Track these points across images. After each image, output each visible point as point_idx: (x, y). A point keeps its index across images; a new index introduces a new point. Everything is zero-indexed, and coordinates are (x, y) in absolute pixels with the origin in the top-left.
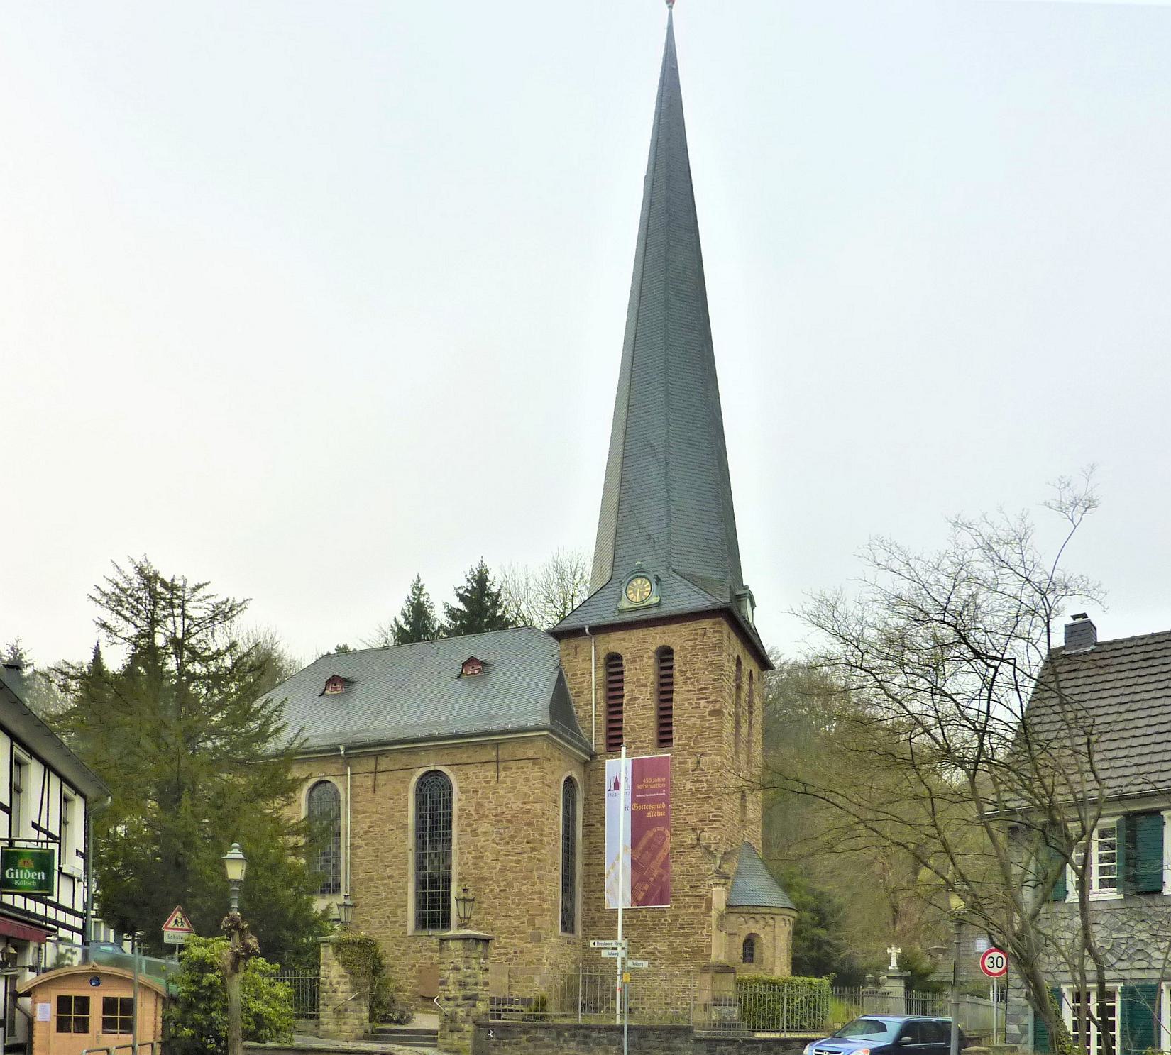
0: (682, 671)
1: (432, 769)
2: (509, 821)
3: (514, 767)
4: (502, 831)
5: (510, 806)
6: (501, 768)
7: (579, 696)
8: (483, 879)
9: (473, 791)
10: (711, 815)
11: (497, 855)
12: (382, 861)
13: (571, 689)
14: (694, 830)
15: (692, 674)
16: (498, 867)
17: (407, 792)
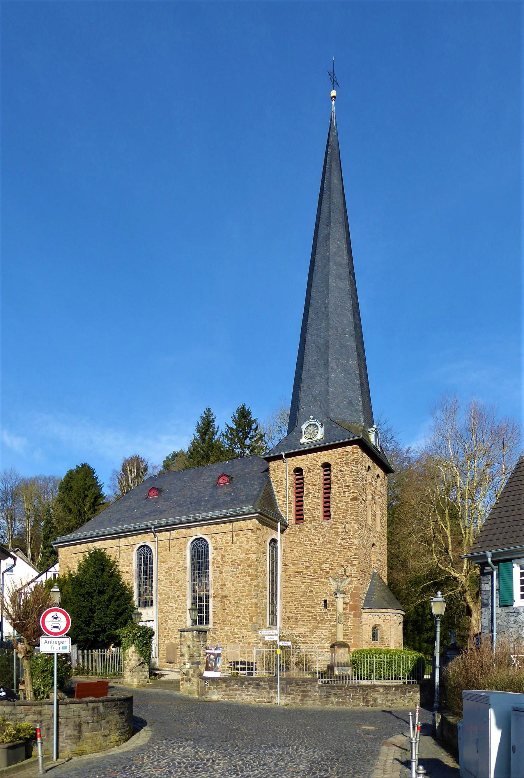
0: (335, 476)
1: (199, 537)
2: (238, 565)
3: (241, 534)
4: (235, 570)
5: (239, 556)
6: (234, 535)
7: (280, 493)
8: (226, 597)
9: (220, 549)
10: (352, 557)
11: (233, 584)
12: (174, 588)
13: (276, 489)
14: (343, 566)
15: (341, 477)
16: (234, 590)
17: (185, 550)
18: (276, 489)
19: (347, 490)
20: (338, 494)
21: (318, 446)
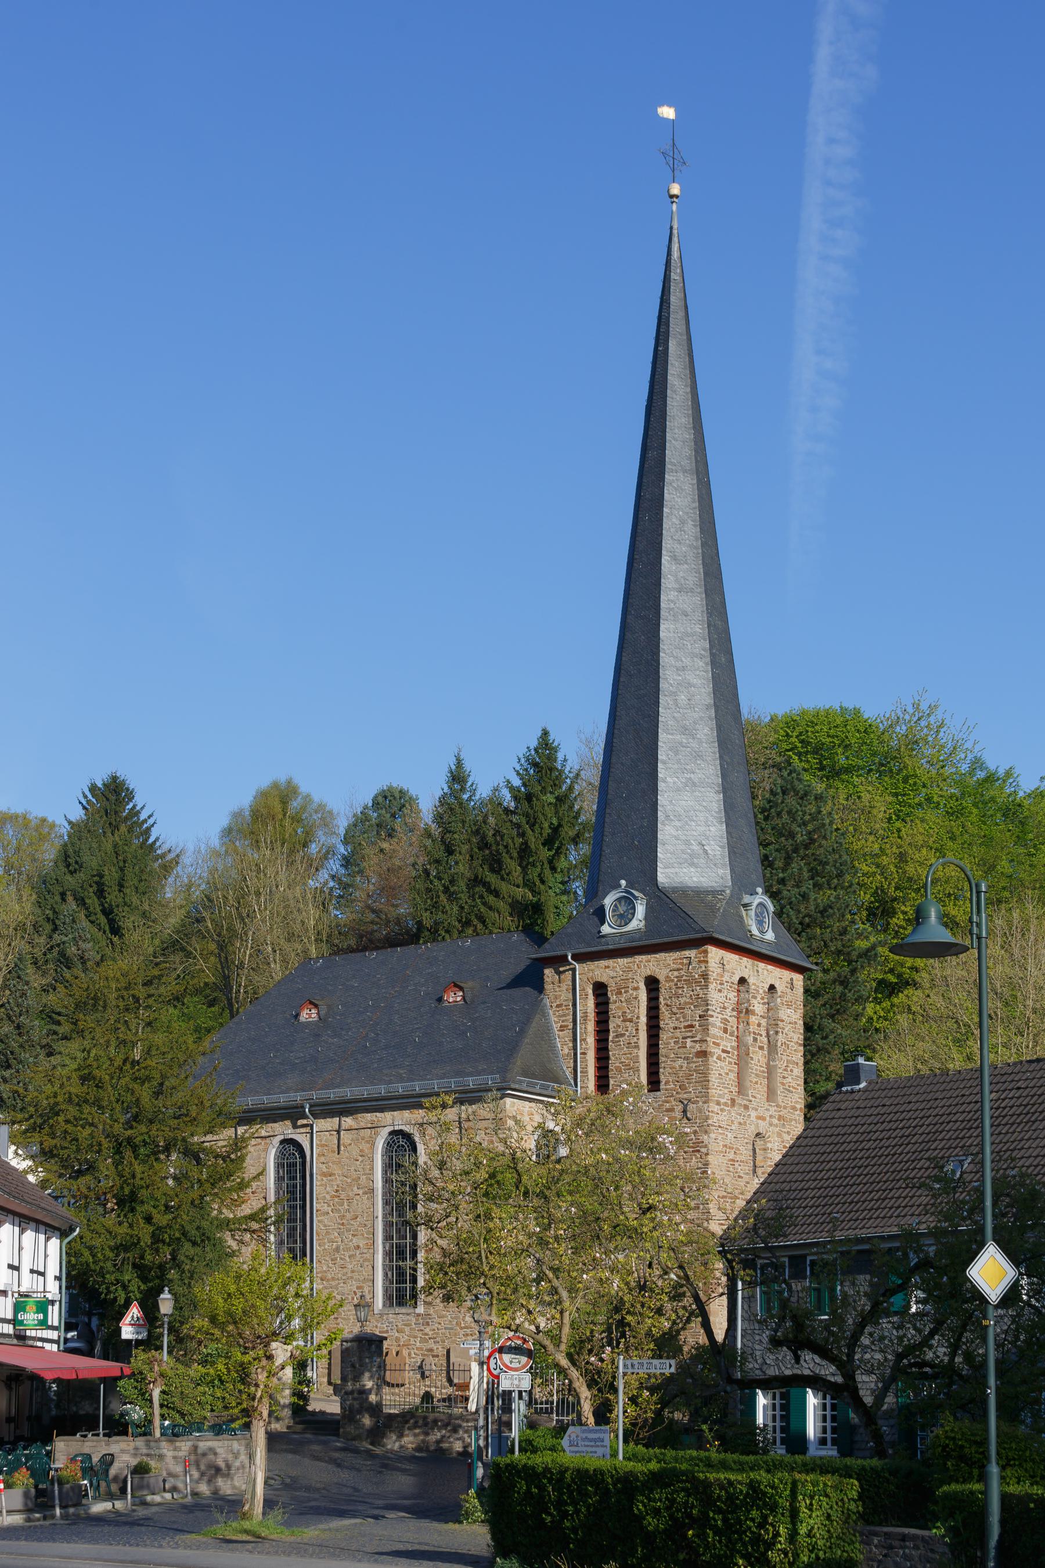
12: (349, 1230)
13: (556, 1023)
18: (556, 1023)
19: (689, 1034)
20: (672, 1041)
21: (634, 944)
